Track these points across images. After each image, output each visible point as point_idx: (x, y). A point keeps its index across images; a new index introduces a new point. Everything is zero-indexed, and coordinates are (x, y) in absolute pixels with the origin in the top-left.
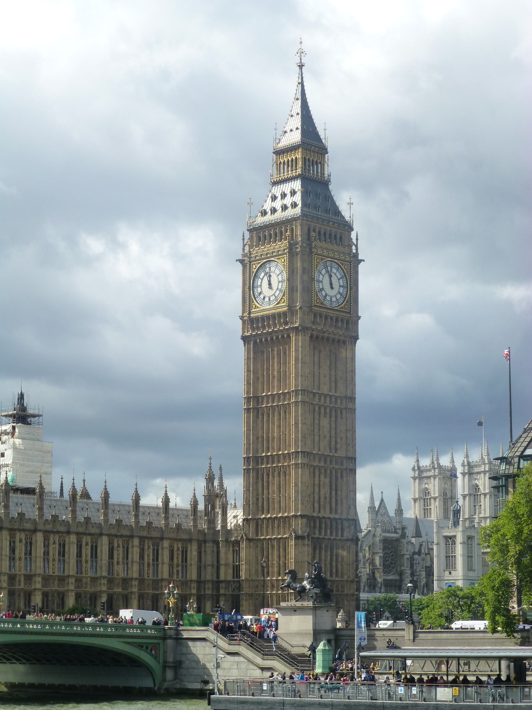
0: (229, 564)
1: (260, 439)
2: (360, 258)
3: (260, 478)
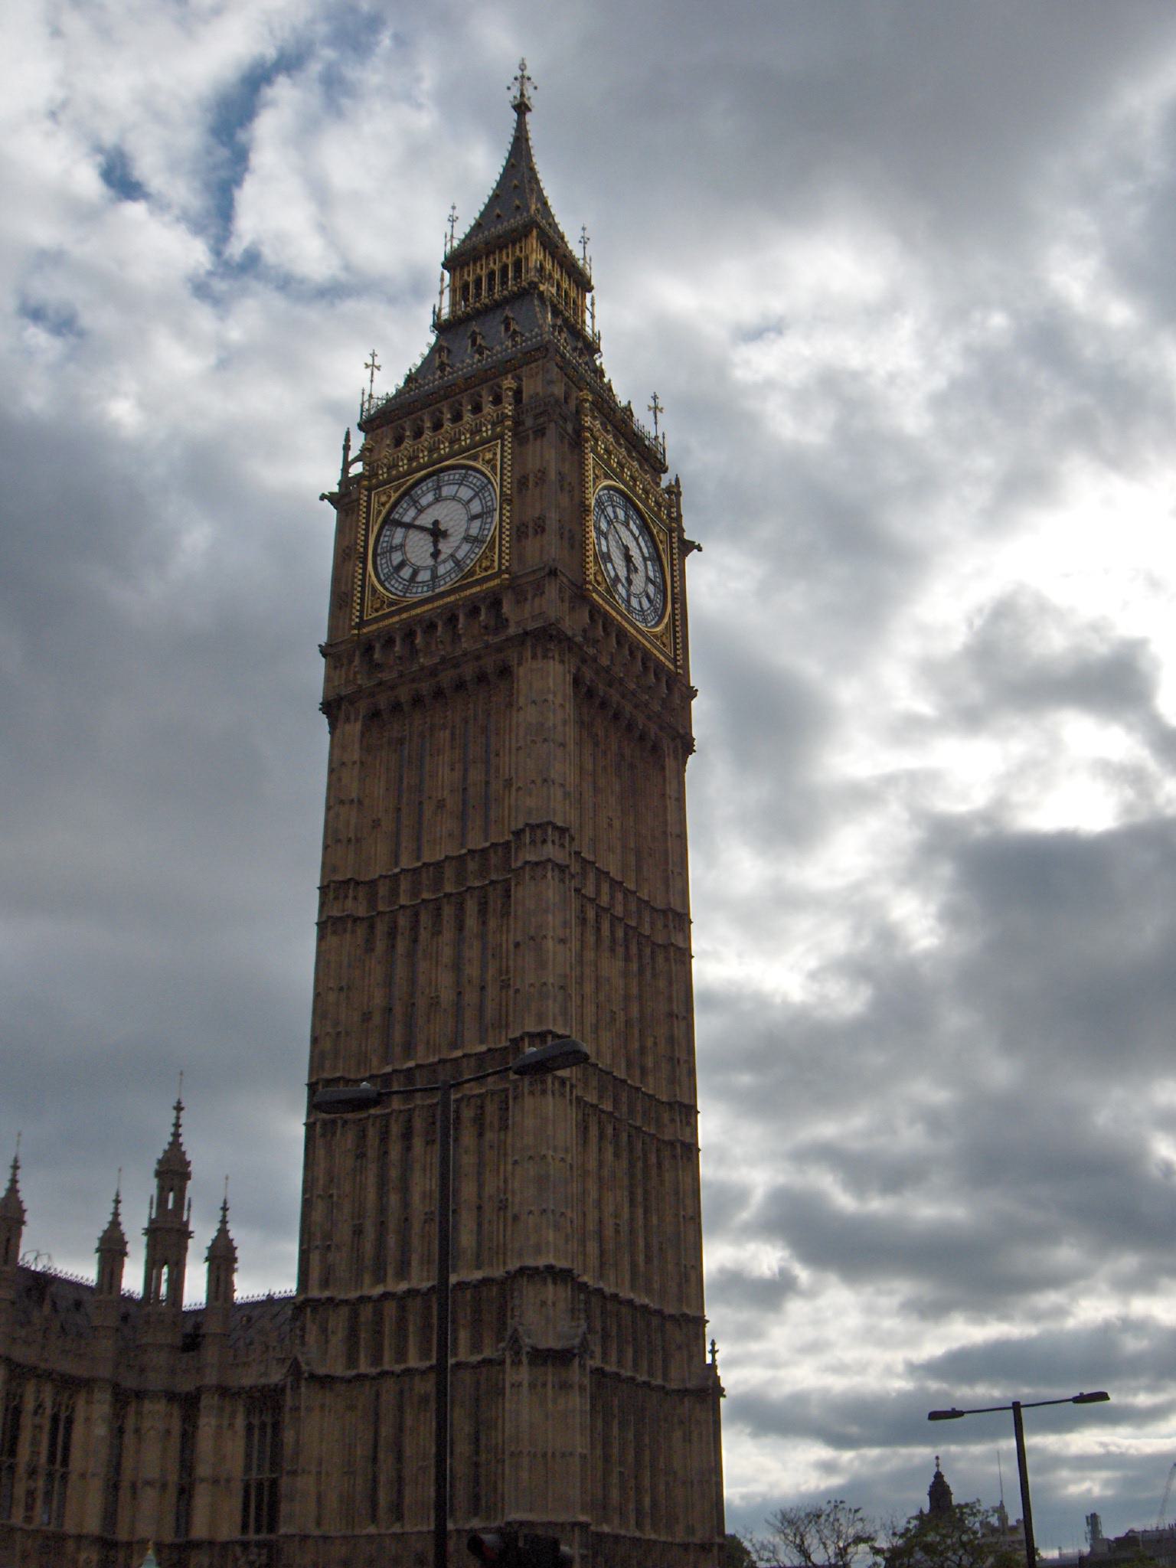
0: (228, 1481)
1: (377, 1019)
2: (687, 536)
3: (371, 1153)
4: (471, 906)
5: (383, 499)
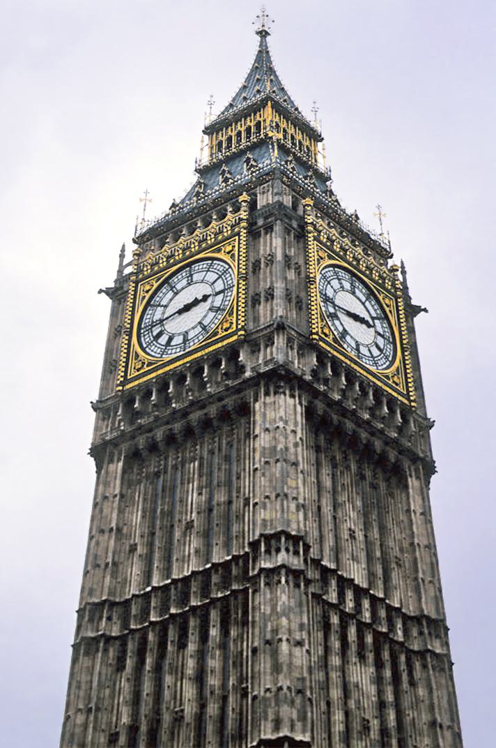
4: (214, 615)
5: (148, 287)
